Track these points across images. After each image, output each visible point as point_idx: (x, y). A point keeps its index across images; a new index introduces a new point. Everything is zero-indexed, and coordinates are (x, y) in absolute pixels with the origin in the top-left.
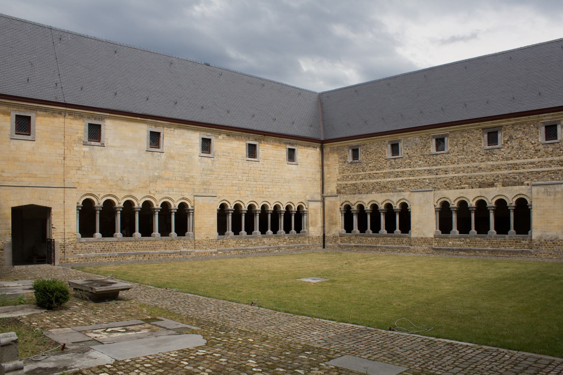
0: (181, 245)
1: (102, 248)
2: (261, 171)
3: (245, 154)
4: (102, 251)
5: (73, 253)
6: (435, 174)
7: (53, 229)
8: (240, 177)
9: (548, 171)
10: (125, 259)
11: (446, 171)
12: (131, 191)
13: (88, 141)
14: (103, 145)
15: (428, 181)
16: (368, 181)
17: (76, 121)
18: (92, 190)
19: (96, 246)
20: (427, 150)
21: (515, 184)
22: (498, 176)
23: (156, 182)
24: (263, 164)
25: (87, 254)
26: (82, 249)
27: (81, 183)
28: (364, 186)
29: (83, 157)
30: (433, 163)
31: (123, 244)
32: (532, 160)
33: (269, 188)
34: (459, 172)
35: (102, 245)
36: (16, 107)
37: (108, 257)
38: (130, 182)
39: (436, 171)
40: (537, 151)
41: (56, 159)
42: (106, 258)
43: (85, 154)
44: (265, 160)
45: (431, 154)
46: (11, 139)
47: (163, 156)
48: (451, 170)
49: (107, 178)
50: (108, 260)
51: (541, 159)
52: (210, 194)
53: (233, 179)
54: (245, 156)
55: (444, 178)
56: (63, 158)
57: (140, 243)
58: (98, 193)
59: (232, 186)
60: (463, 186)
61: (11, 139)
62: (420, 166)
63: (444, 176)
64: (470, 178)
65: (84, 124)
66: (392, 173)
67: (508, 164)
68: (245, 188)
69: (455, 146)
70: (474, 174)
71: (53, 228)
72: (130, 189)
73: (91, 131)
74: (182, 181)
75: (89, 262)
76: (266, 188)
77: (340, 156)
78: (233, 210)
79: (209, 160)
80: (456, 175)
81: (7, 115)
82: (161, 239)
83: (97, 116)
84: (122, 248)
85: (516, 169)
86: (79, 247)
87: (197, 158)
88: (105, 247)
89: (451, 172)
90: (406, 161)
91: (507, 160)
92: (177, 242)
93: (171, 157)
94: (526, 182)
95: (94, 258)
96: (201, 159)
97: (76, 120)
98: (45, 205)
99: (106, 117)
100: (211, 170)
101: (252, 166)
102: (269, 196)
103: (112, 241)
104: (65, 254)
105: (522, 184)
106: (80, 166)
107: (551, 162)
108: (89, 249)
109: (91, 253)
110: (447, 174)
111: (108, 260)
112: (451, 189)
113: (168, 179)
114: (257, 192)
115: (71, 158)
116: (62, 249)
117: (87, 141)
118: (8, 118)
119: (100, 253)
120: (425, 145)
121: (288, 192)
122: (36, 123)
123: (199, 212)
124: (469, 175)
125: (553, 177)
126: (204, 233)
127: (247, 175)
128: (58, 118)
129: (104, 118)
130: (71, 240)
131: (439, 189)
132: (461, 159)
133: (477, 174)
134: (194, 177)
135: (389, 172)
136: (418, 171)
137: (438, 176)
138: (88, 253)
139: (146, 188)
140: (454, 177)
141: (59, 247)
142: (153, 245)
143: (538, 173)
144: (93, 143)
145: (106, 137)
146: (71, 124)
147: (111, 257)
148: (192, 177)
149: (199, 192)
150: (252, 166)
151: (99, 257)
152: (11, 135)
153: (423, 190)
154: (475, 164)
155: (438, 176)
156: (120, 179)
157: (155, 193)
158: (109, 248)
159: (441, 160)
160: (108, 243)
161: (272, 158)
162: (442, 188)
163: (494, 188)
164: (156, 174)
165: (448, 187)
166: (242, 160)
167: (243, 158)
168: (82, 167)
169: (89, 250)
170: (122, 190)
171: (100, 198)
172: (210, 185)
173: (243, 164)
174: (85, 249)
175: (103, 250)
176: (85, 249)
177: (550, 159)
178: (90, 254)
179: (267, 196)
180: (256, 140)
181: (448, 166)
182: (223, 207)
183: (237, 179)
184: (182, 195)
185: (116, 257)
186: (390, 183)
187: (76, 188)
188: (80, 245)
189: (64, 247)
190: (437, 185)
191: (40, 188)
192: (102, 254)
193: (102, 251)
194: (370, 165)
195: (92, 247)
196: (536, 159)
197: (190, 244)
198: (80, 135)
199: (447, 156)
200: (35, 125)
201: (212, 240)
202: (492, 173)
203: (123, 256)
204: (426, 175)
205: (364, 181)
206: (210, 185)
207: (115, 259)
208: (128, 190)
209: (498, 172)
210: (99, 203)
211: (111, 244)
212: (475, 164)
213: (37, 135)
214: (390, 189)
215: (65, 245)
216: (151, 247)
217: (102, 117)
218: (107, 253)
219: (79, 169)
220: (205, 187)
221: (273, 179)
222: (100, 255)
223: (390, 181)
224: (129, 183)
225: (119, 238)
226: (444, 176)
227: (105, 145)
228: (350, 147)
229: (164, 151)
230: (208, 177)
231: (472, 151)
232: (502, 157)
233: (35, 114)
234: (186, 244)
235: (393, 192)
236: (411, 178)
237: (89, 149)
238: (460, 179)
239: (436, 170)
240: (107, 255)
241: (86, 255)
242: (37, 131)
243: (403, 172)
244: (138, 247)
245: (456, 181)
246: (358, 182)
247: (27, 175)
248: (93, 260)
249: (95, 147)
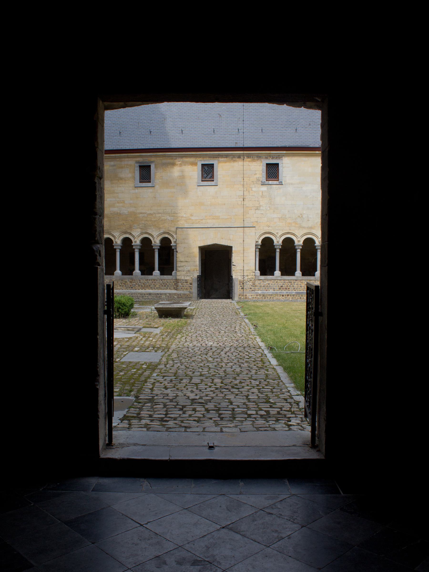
1: (280, 286)
4: (280, 289)
5: (251, 290)
7: (233, 266)
12: (311, 228)
13: (266, 180)
14: (281, 184)
17: (254, 163)
18: (270, 228)
19: (274, 284)
25: (265, 291)
26: (260, 286)
27: (260, 222)
29: (262, 197)
31: (302, 283)
35: (280, 283)
36: (202, 157)
37: (286, 296)
38: (310, 219)
41: (236, 201)
42: (283, 296)
43: (263, 194)
46: (198, 186)
49: (286, 216)
50: (285, 298)
56: (242, 200)
58: (277, 232)
61: (198, 186)
65: (261, 164)
71: (233, 265)
72: (310, 226)
73: (270, 171)
75: (266, 299)
81: (195, 165)
83: (275, 155)
84: (301, 287)
86: (258, 285)
88: (284, 286)
95: (271, 295)
97: (254, 161)
98: (226, 244)
99: (284, 155)
103: (291, 280)
104: (243, 290)
106: (258, 205)
108: (267, 286)
109: (269, 290)
111: (285, 298)
115: (250, 199)
116: (241, 285)
117: (265, 181)
118: (195, 168)
119: (278, 291)
122: (218, 169)
128: (237, 162)
129: (282, 156)
130: (250, 277)
138: (266, 290)
141: (239, 283)
144: (270, 182)
145: (284, 175)
146: (249, 166)
147: (288, 295)
151: (277, 294)
152: (198, 183)
156: (299, 216)
158: (287, 286)
160: (286, 281)
168: (260, 206)
169: (267, 287)
170: (301, 227)
171: (278, 236)
174: (263, 287)
175: (281, 288)
176: (263, 287)
178: (268, 291)
185: (293, 295)
187: (255, 227)
188: (259, 282)
189: (243, 284)
191: (222, 228)
192: (280, 292)
193: (280, 289)
195: (270, 285)
198: (258, 176)
200: (217, 171)
203: (301, 295)
207: (292, 298)
208: (308, 228)
210: (278, 241)
211: (290, 282)
213: (219, 180)
215: (244, 281)
217: (279, 155)
218: (285, 292)
219: (257, 209)
222: (277, 293)
224: (309, 220)
227: (283, 184)
233: (217, 161)
237: (267, 189)
240: (285, 293)
241: (263, 292)
242: (219, 176)
247: (211, 217)
248: (270, 298)
249: (273, 186)
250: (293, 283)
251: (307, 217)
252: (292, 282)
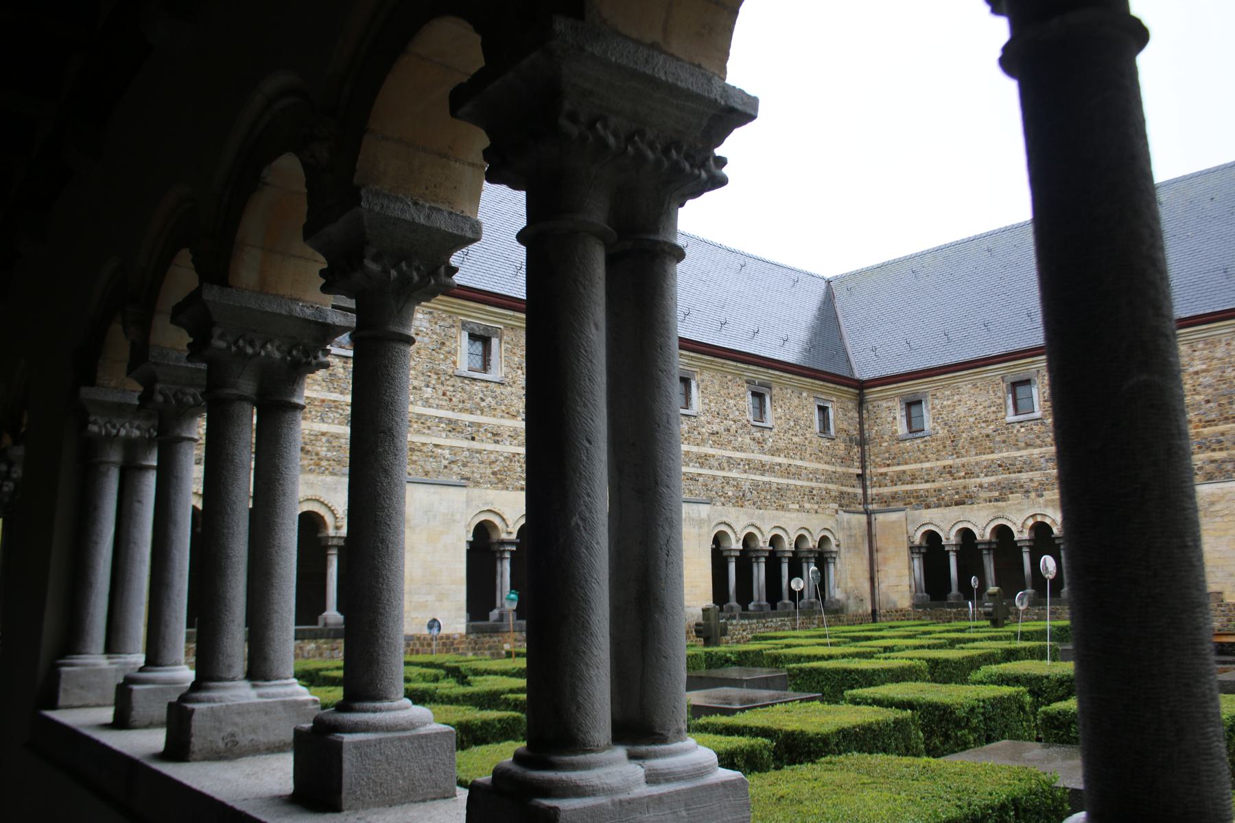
6: (470, 437)
11: (495, 435)
15: (447, 452)
20: (446, 358)
30: (463, 402)
39: (469, 429)
45: (457, 373)
48: (509, 433)
55: (491, 452)
63: (491, 447)
89: (509, 439)
110: (497, 442)
112: (507, 488)
120: (443, 344)
131: (477, 484)
135: (323, 401)
136: (419, 416)
137: (476, 445)
153: (435, 479)
155: (476, 445)
159: (483, 400)
162: (485, 483)
165: (501, 481)
186: (324, 439)
190: (473, 472)
199: (498, 390)
204: (444, 435)
214: (324, 463)
223: (323, 434)
226: (491, 447)
235: (333, 474)
239: (472, 424)
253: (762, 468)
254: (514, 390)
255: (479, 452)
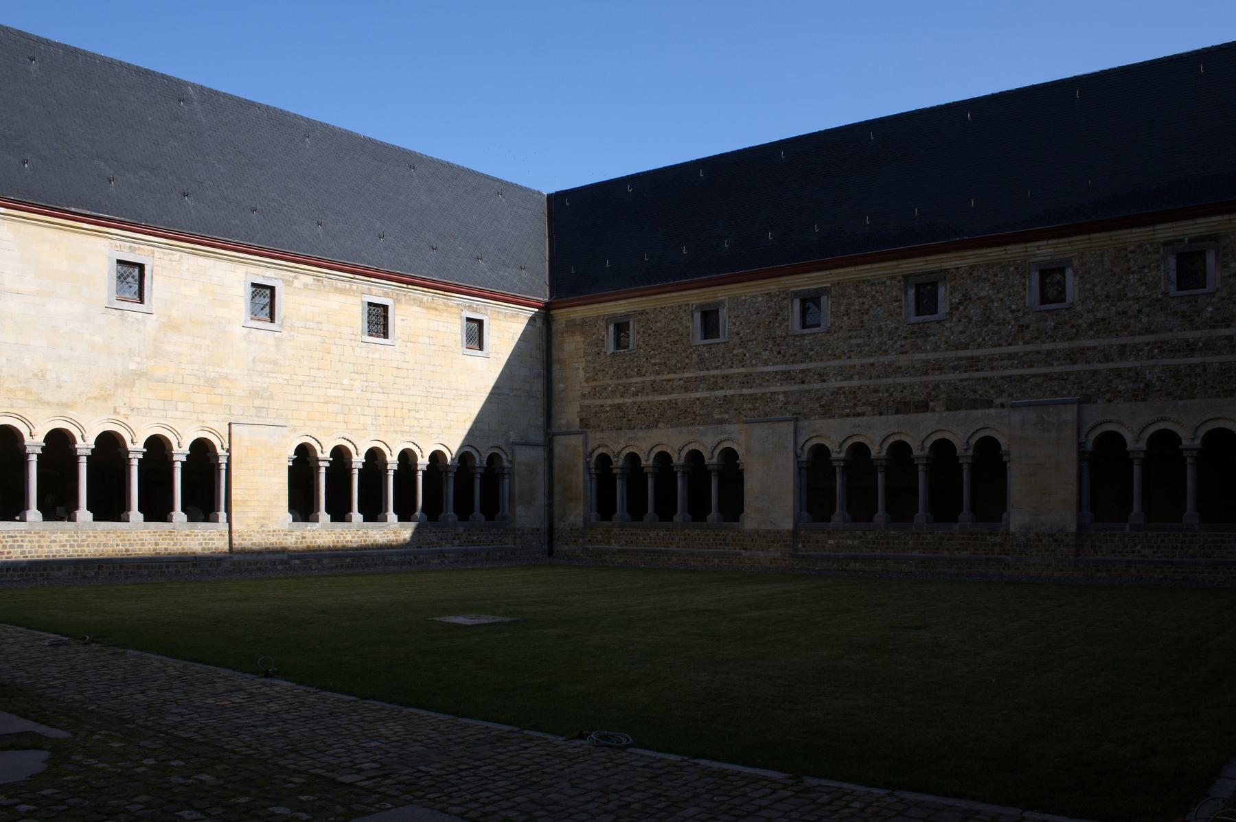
0: (197, 543)
2: (398, 368)
3: (360, 328)
8: (346, 382)
9: (1045, 375)
10: (48, 575)
12: (66, 405)
15: (781, 397)
16: (650, 398)
21: (974, 405)
22: (937, 387)
23: (133, 386)
24: (404, 354)
28: (641, 410)
32: (1013, 349)
33: (417, 411)
34: (851, 378)
38: (62, 384)
39: (800, 375)
40: (1023, 328)
44: (409, 344)
47: (152, 323)
51: (1029, 348)
52: (272, 420)
53: (328, 385)
54: (360, 332)
55: (819, 390)
57: (90, 536)
59: (327, 403)
60: (859, 409)
62: (766, 363)
63: (817, 386)
64: (876, 391)
66: (703, 379)
67: (960, 359)
68: (359, 409)
69: (844, 315)
70: (884, 381)
72: (64, 401)
74: (199, 386)
76: (410, 410)
77: (588, 341)
78: (330, 462)
79: (270, 339)
80: (846, 384)
82: (146, 528)
85: (977, 370)
87: (239, 331)
90: (735, 352)
91: (957, 349)
92: (188, 535)
93: (172, 326)
94: (998, 401)
96: (250, 332)
100: (275, 363)
101: (377, 356)
102: (419, 429)
105: (990, 404)
107: (1050, 353)
110: (824, 381)
113: (163, 381)
114: (389, 418)
120: (778, 314)
121: (465, 421)
123: (241, 462)
124: (872, 383)
125: (1056, 388)
126: (256, 515)
127: (363, 377)
131: (807, 417)
132: (858, 345)
133: (890, 380)
134: (229, 377)
137: (805, 387)
139: (105, 400)
140: (840, 389)
142: (124, 540)
143: (1023, 379)
148: (226, 377)
149: (242, 415)
150: (377, 356)
154: (886, 359)
155: (805, 387)
156: (36, 375)
157: (130, 413)
161: (427, 340)
163: (929, 415)
164: (133, 366)
166: (351, 340)
167: (353, 337)
170: (39, 402)
172: (271, 397)
173: (353, 349)
177: (1049, 346)
179: (412, 430)
180: (386, 295)
181: (829, 363)
182: (304, 454)
183: (339, 386)
184: (198, 420)
194: (653, 361)
196: (1019, 348)
197: (219, 539)
201: (274, 531)
202: (925, 378)
204: (779, 384)
205: (639, 399)
206: (271, 397)
208: (58, 404)
209: (935, 377)
211: (12, 537)
212: (886, 359)
216: (117, 545)
220: (257, 403)
221: (429, 389)
223: (698, 399)
224: (60, 387)
225: (32, 523)
226: (817, 386)
228: (609, 319)
229: (153, 311)
230: (267, 380)
231: (880, 329)
232: (946, 343)
234: (209, 540)
236: (745, 391)
238: (853, 392)
239: (802, 371)
243: (726, 377)
244: (83, 546)
245: (846, 397)
246: (629, 400)
250: (20, 539)
251: (57, 378)
252: (16, 536)
253: (1190, 348)
254: (840, 335)
255: (809, 391)
